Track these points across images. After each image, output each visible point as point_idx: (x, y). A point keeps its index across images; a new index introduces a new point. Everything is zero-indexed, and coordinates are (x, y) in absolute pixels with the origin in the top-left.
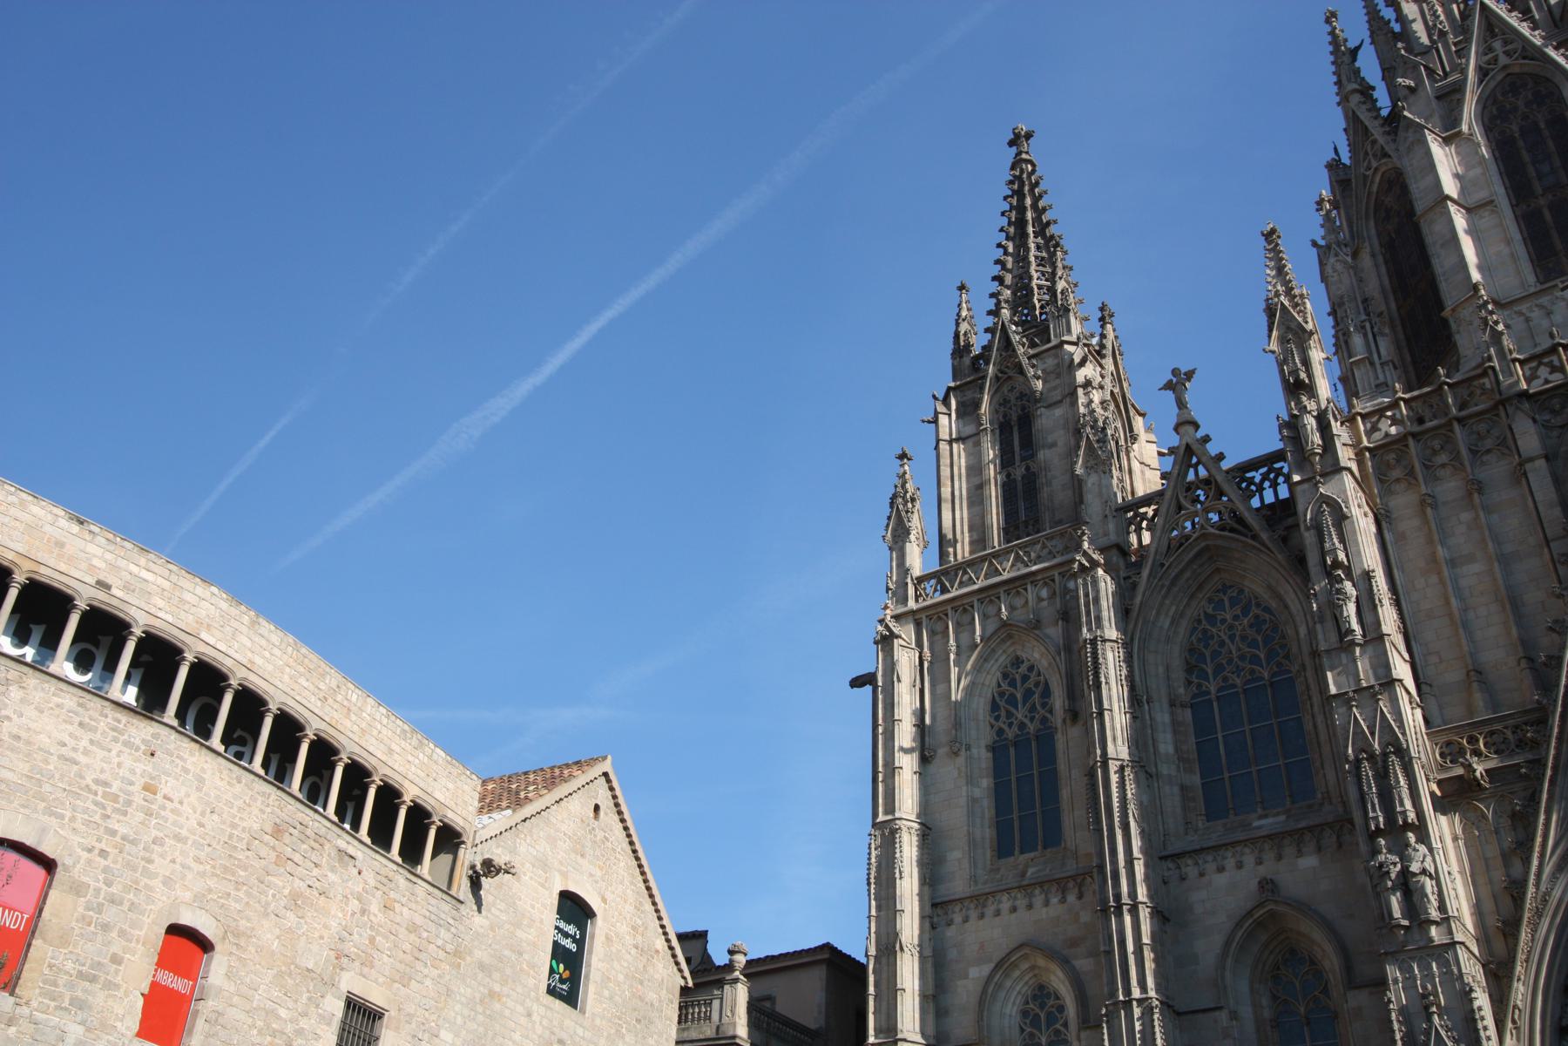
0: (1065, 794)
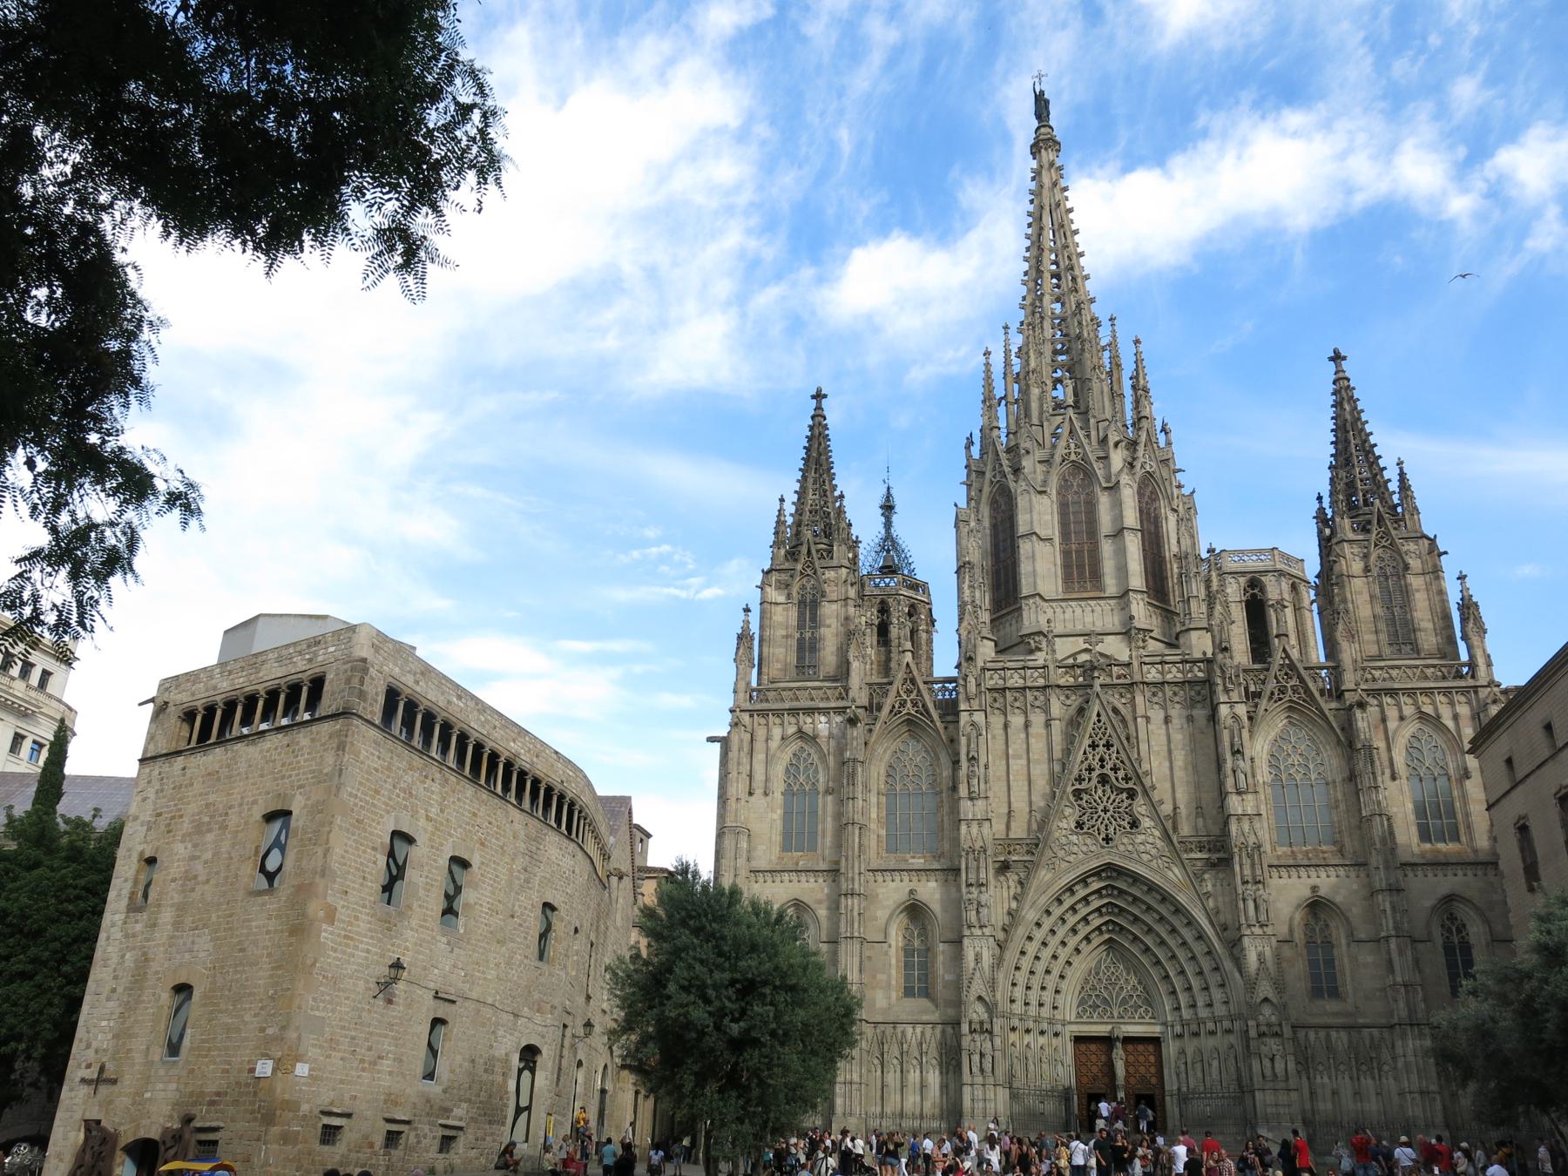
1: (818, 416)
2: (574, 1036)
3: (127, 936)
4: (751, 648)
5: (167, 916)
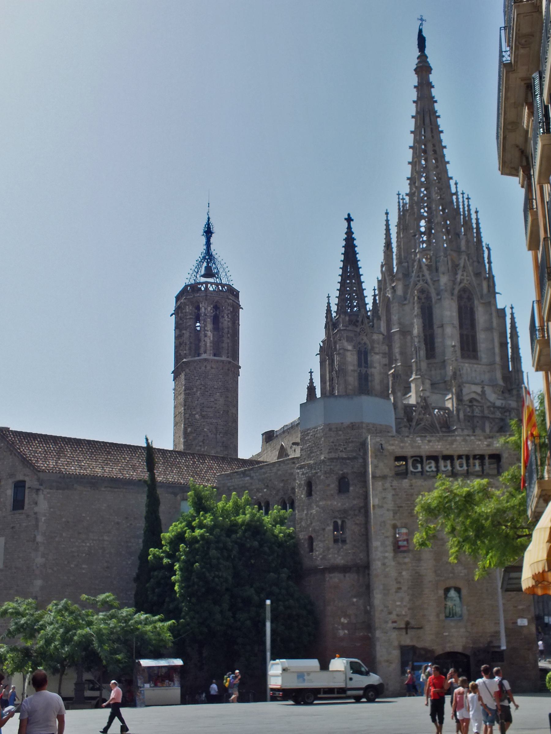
1: (349, 232)
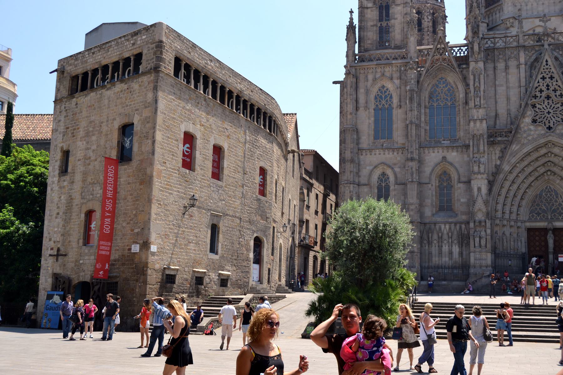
0: (395, 126)
2: (277, 232)
3: (60, 188)
4: (355, 33)
5: (78, 177)
